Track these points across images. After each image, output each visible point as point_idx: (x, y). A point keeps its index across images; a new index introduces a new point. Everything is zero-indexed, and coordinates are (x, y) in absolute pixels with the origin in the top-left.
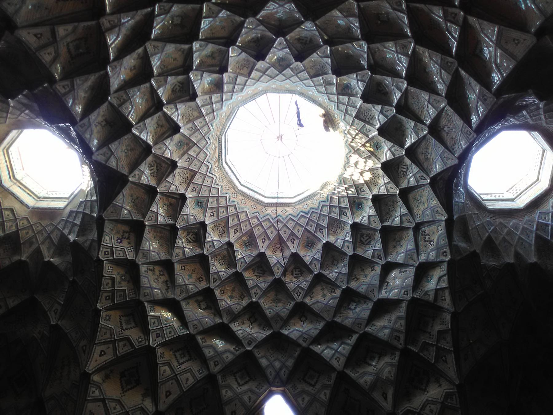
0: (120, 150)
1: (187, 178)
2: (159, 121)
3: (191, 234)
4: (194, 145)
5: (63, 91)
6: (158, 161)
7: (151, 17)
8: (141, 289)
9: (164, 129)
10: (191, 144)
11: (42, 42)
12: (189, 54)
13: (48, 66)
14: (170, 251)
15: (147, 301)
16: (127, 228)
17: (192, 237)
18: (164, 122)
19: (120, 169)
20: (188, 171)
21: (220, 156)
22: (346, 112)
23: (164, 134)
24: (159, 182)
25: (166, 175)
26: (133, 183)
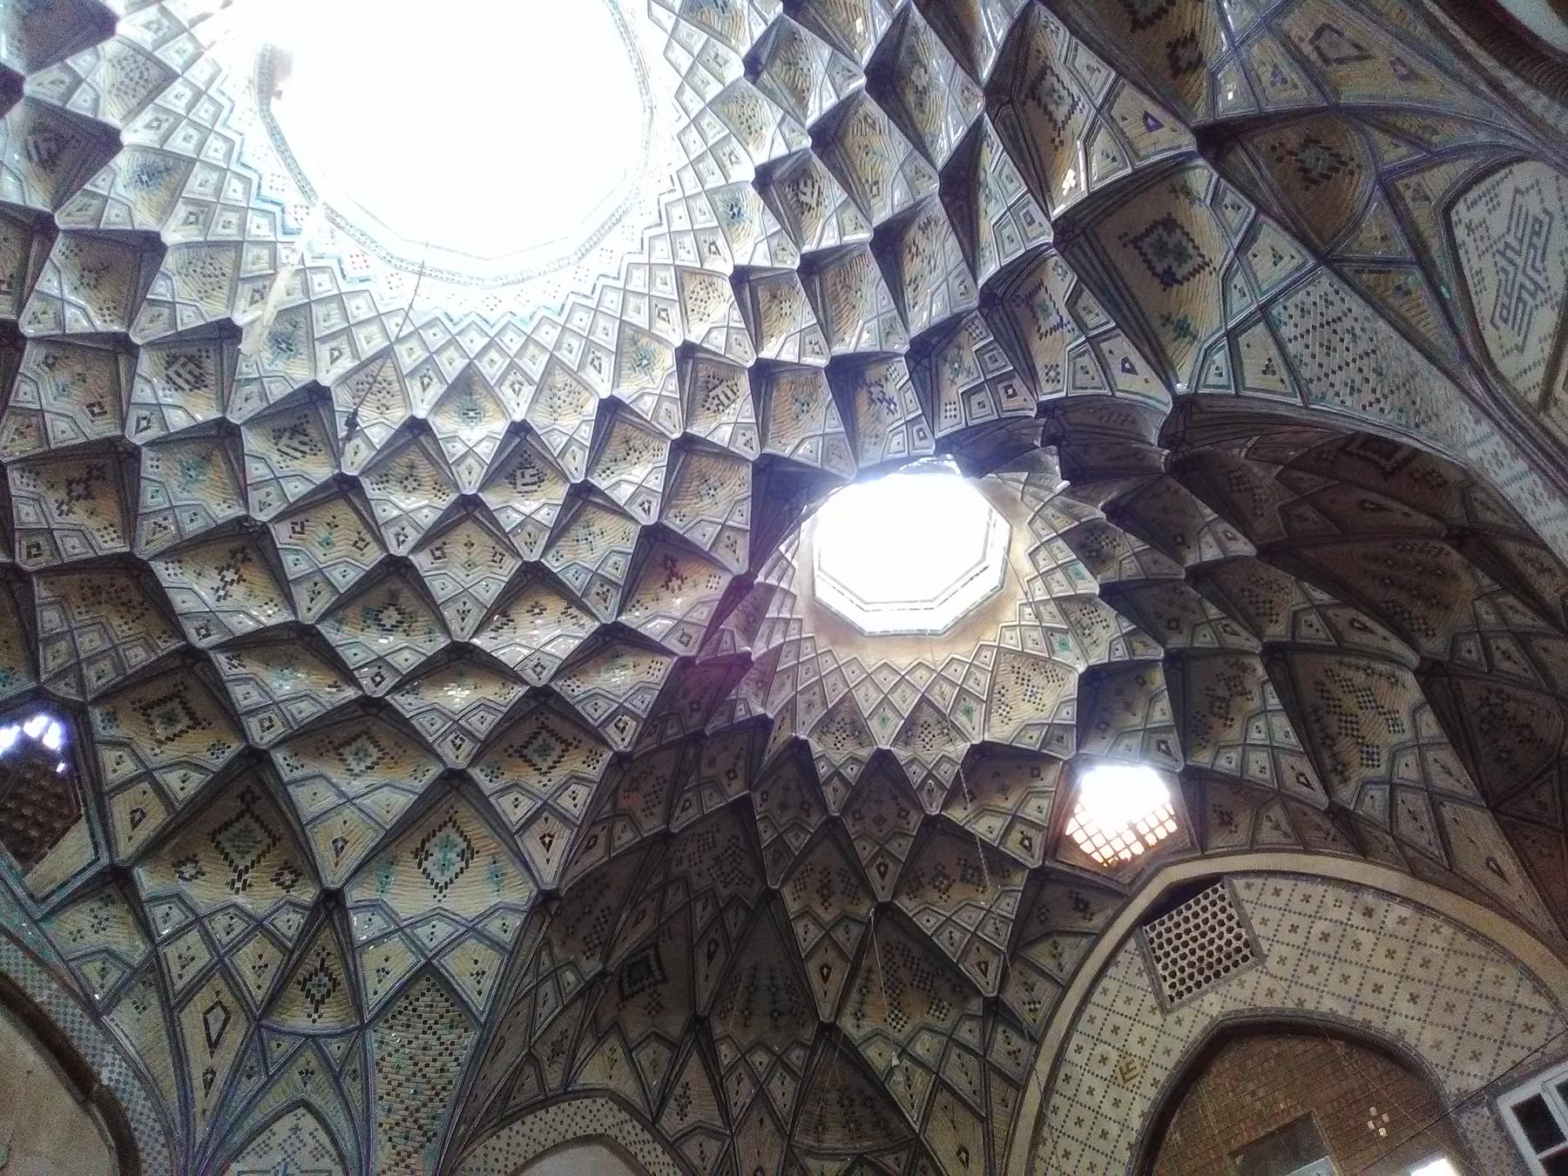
0: (715, 510)
2: (620, 456)
3: (803, 198)
5: (632, 724)
6: (700, 396)
7: (410, 681)
8: (956, 310)
10: (629, 331)
11: (555, 826)
12: (435, 537)
14: (855, 254)
15: (975, 280)
16: (862, 398)
17: (808, 190)
18: (615, 447)
19: (747, 491)
20: (687, 294)
22: (198, 95)
23: (635, 426)
24: (735, 368)
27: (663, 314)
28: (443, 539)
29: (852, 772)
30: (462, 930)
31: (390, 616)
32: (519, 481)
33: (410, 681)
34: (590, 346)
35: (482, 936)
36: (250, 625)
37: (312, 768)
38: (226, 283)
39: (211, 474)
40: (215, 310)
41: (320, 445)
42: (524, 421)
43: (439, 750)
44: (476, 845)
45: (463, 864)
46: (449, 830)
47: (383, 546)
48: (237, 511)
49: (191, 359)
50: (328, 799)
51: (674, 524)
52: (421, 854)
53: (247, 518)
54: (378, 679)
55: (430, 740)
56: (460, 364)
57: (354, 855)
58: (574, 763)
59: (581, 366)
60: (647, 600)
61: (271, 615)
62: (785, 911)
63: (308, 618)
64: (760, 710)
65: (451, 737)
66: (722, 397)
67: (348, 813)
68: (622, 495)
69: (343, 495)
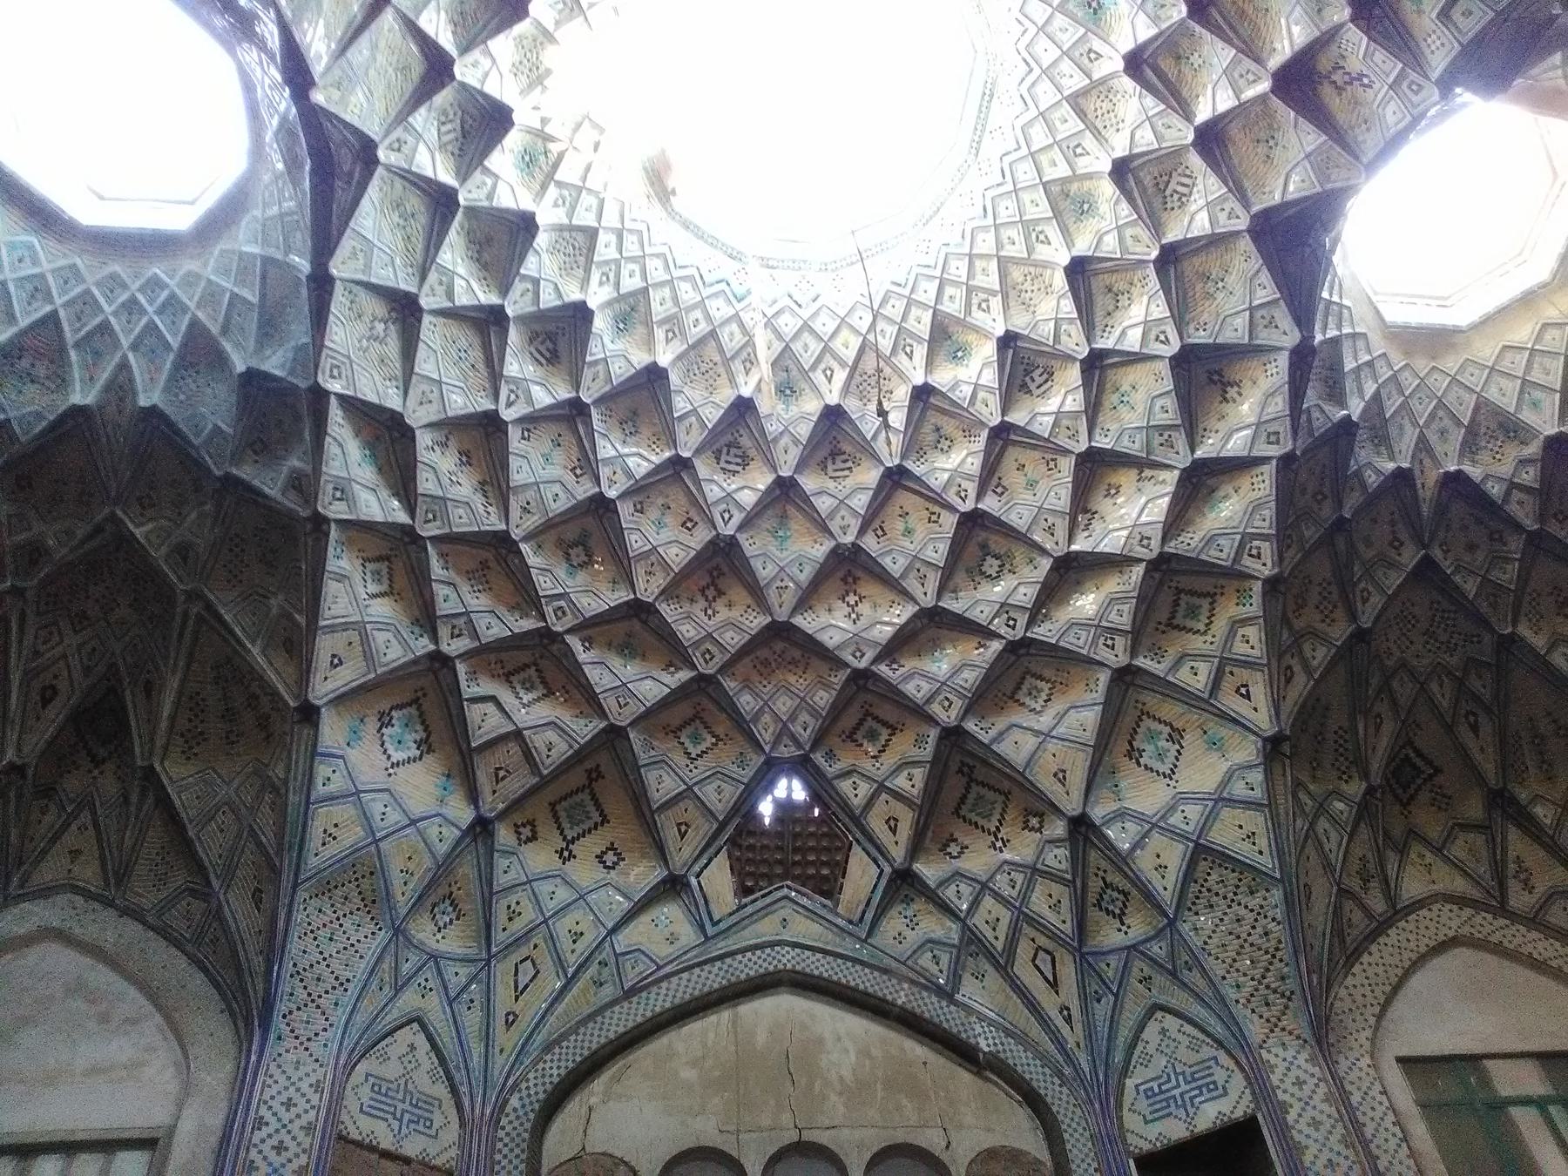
0: (1233, 299)
1: (1102, 97)
2: (1111, 308)
4: (1048, 182)
7: (1036, 613)
9: (1108, 279)
10: (1055, 189)
11: (1243, 675)
12: (989, 476)
13: (1261, 621)
18: (1102, 302)
19: (1256, 262)
21: (987, 98)
22: (620, 235)
23: (1112, 271)
24: (1177, 153)
25: (1154, 156)
26: (1246, 205)
27: (1079, 151)
28: (997, 475)
29: (1529, 476)
30: (1211, 804)
31: (991, 566)
32: (1032, 386)
33: (1036, 613)
34: (1028, 227)
35: (1232, 802)
36: (889, 631)
37: (1001, 723)
38: (721, 370)
39: (794, 525)
40: (725, 397)
41: (858, 455)
42: (1007, 331)
43: (1097, 658)
44: (1178, 725)
45: (1178, 747)
46: (1148, 723)
47: (950, 508)
48: (829, 545)
49: (729, 446)
50: (1030, 742)
51: (1200, 337)
52: (1133, 754)
53: (838, 546)
54: (1011, 623)
55: (1084, 652)
56: (927, 317)
57: (1077, 778)
58: (1229, 610)
59: (1030, 250)
60: (1212, 423)
61: (899, 614)
62: (1532, 649)
63: (928, 601)
64: (1391, 466)
65: (1102, 640)
66: (1180, 189)
67: (1052, 746)
68: (1133, 341)
69: (897, 485)
